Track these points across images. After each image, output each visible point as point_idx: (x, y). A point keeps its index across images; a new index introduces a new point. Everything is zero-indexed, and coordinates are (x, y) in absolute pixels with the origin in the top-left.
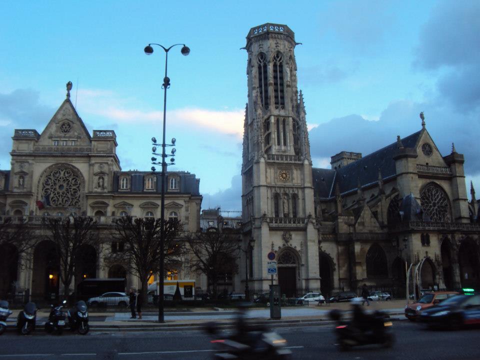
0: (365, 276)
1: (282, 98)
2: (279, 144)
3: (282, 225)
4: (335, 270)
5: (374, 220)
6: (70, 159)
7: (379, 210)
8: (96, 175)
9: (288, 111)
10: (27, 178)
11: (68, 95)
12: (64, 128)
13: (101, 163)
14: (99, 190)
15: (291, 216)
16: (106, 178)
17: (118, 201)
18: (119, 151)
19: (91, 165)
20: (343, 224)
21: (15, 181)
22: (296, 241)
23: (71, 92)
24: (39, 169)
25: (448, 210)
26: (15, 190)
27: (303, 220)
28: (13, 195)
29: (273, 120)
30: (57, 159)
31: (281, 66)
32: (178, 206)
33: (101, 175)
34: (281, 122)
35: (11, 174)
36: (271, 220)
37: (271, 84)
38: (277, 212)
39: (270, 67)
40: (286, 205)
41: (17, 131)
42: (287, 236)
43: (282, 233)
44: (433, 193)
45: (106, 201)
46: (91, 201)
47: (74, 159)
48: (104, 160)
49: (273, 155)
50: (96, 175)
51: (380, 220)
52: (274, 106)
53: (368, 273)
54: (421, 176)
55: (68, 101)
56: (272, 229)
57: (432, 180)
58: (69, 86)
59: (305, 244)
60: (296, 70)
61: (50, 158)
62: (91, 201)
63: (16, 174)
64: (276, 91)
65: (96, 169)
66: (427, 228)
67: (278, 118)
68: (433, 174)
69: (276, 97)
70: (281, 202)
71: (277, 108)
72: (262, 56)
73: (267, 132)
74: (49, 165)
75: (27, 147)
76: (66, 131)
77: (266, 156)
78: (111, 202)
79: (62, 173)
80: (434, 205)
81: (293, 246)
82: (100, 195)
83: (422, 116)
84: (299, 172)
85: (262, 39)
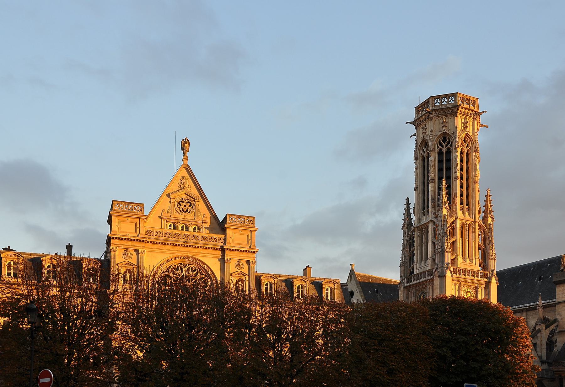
6: (196, 250)
12: (183, 206)
30: (177, 248)
47: (202, 251)
49: (460, 270)
61: (168, 247)
74: (167, 256)
76: (185, 210)
85: (446, 115)
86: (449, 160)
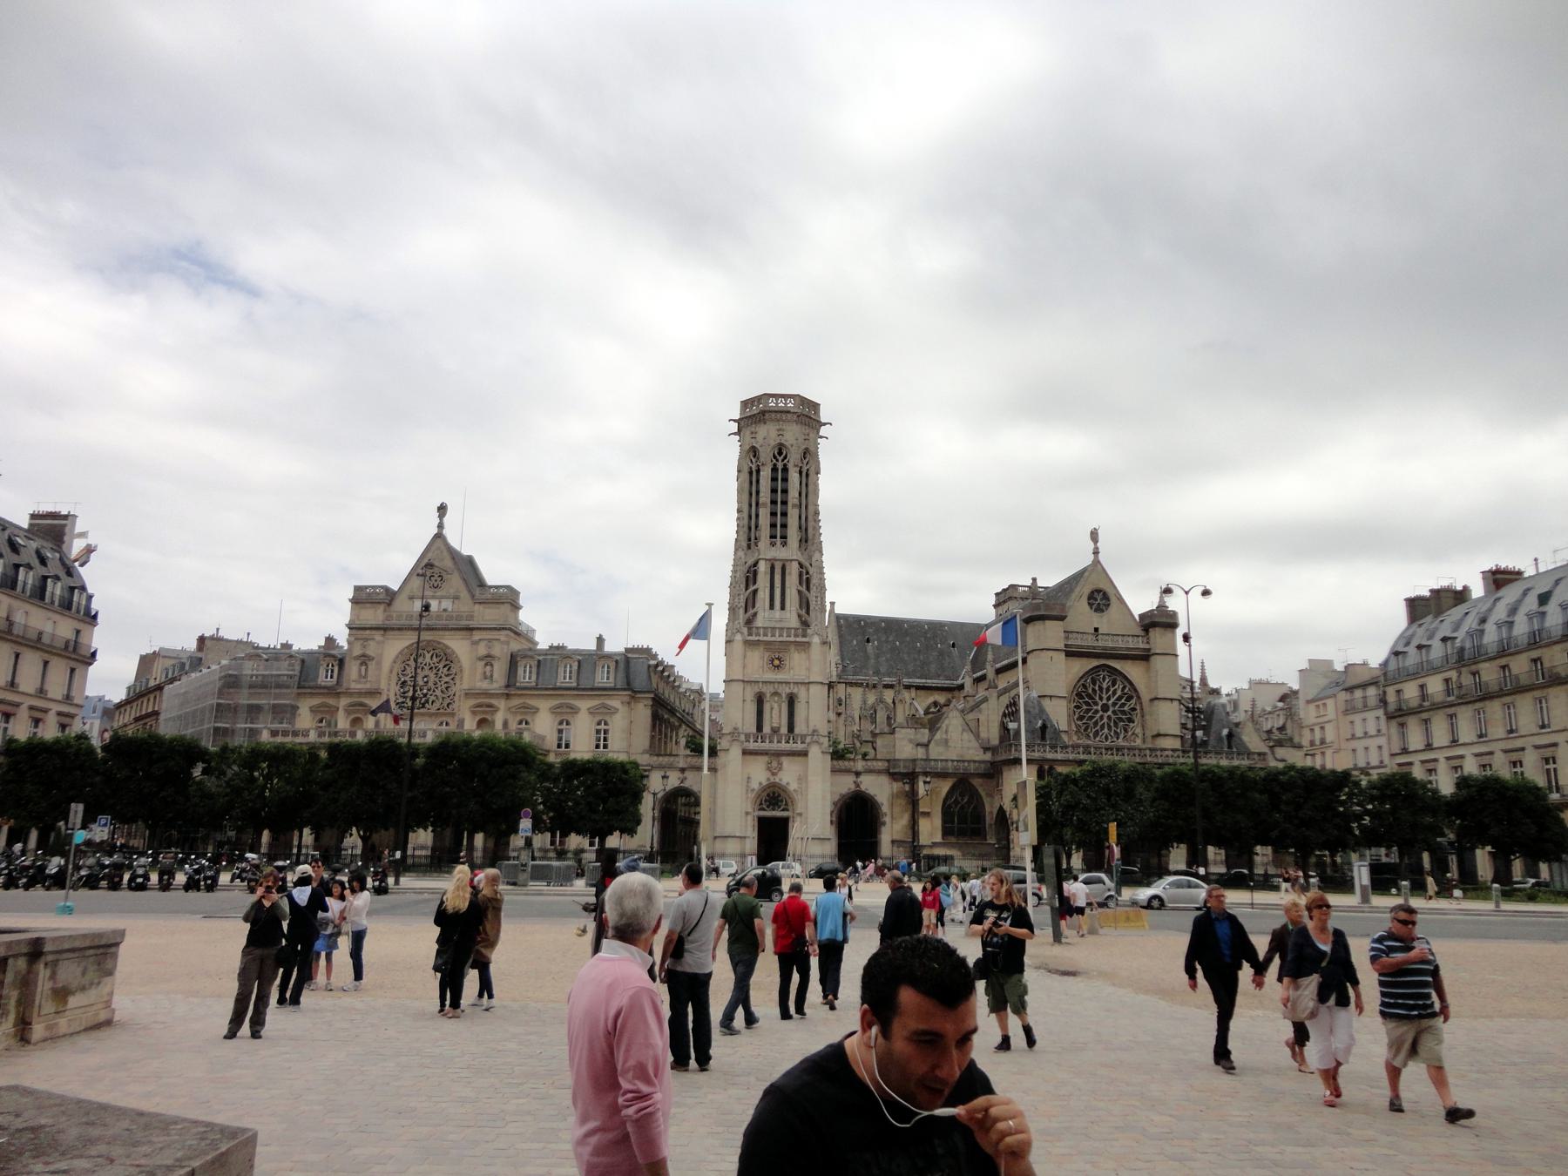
0: (938, 839)
1: (784, 526)
2: (772, 607)
3: (766, 746)
4: (884, 824)
5: (967, 736)
7: (982, 718)
8: (481, 659)
9: (791, 551)
10: (372, 666)
11: (441, 526)
13: (490, 640)
14: (485, 685)
15: (784, 730)
16: (496, 667)
17: (515, 702)
18: (526, 616)
20: (905, 742)
21: (352, 670)
22: (789, 775)
23: (445, 520)
24: (393, 649)
25: (1137, 719)
26: (353, 685)
27: (803, 737)
28: (348, 693)
31: (785, 469)
32: (612, 711)
33: (488, 659)
34: (778, 569)
35: (347, 660)
36: (747, 736)
37: (765, 505)
38: (760, 728)
39: (766, 474)
40: (776, 712)
41: (357, 589)
42: (774, 764)
43: (766, 758)
44: (1105, 686)
45: (494, 702)
46: (472, 702)
48: (494, 635)
50: (481, 659)
51: (983, 735)
52: (768, 540)
53: (946, 832)
54: (1071, 653)
55: (439, 536)
56: (745, 752)
57: (1103, 662)
58: (442, 509)
59: (803, 779)
60: (818, 473)
62: (472, 702)
63: (356, 658)
64: (773, 514)
65: (482, 650)
66: (1050, 756)
68: (1105, 648)
69: (773, 526)
70: (767, 707)
71: (773, 545)
72: (754, 451)
73: (752, 588)
74: (407, 643)
75: (374, 616)
77: (745, 630)
78: (501, 704)
79: (428, 656)
80: (1105, 708)
81: (784, 782)
82: (486, 694)
83: (1094, 536)
84: (803, 655)
86: (785, 480)
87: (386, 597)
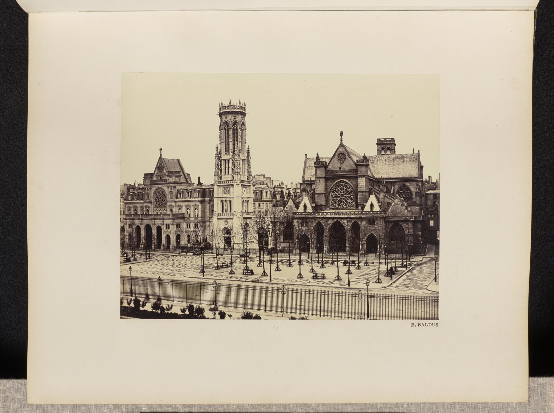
11: (161, 155)
15: (229, 212)
19: (168, 188)
29: (222, 161)
41: (145, 174)
43: (224, 220)
67: (225, 160)
87: (152, 175)
